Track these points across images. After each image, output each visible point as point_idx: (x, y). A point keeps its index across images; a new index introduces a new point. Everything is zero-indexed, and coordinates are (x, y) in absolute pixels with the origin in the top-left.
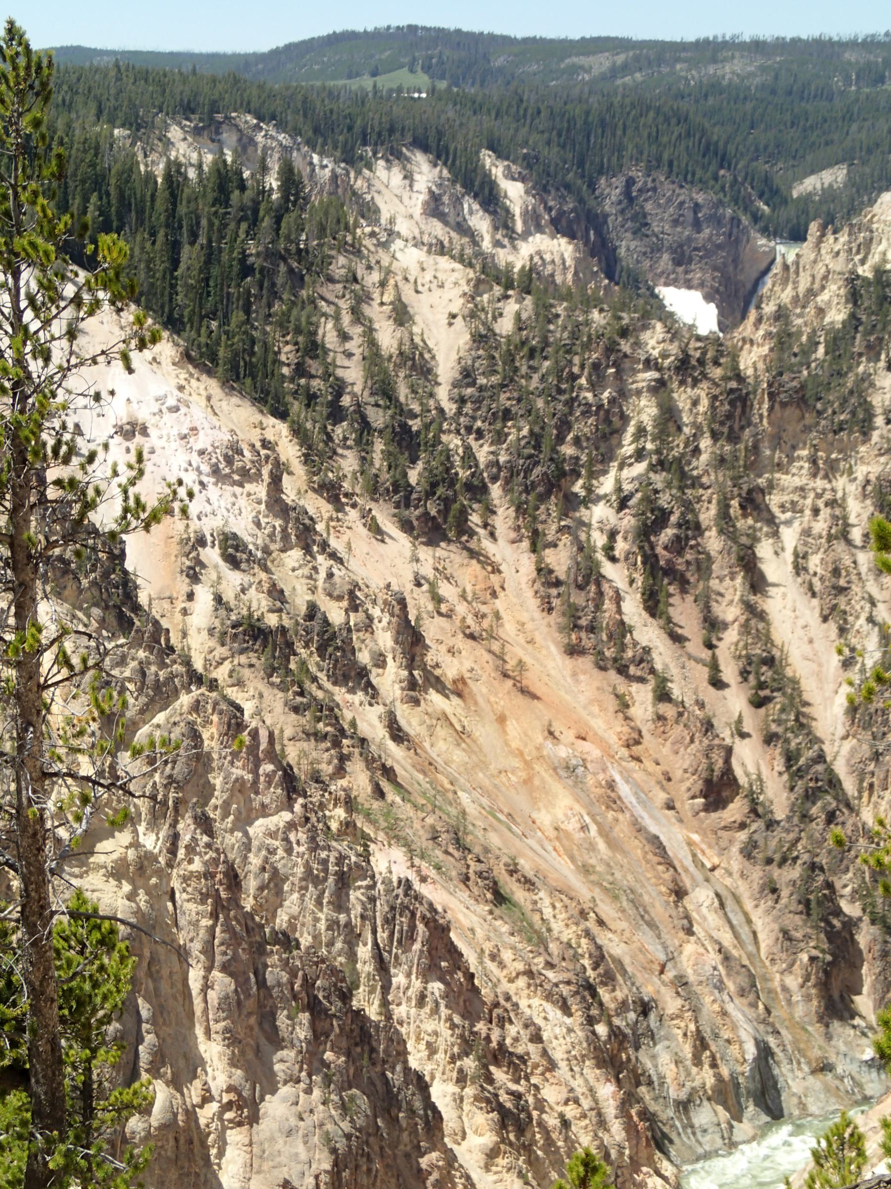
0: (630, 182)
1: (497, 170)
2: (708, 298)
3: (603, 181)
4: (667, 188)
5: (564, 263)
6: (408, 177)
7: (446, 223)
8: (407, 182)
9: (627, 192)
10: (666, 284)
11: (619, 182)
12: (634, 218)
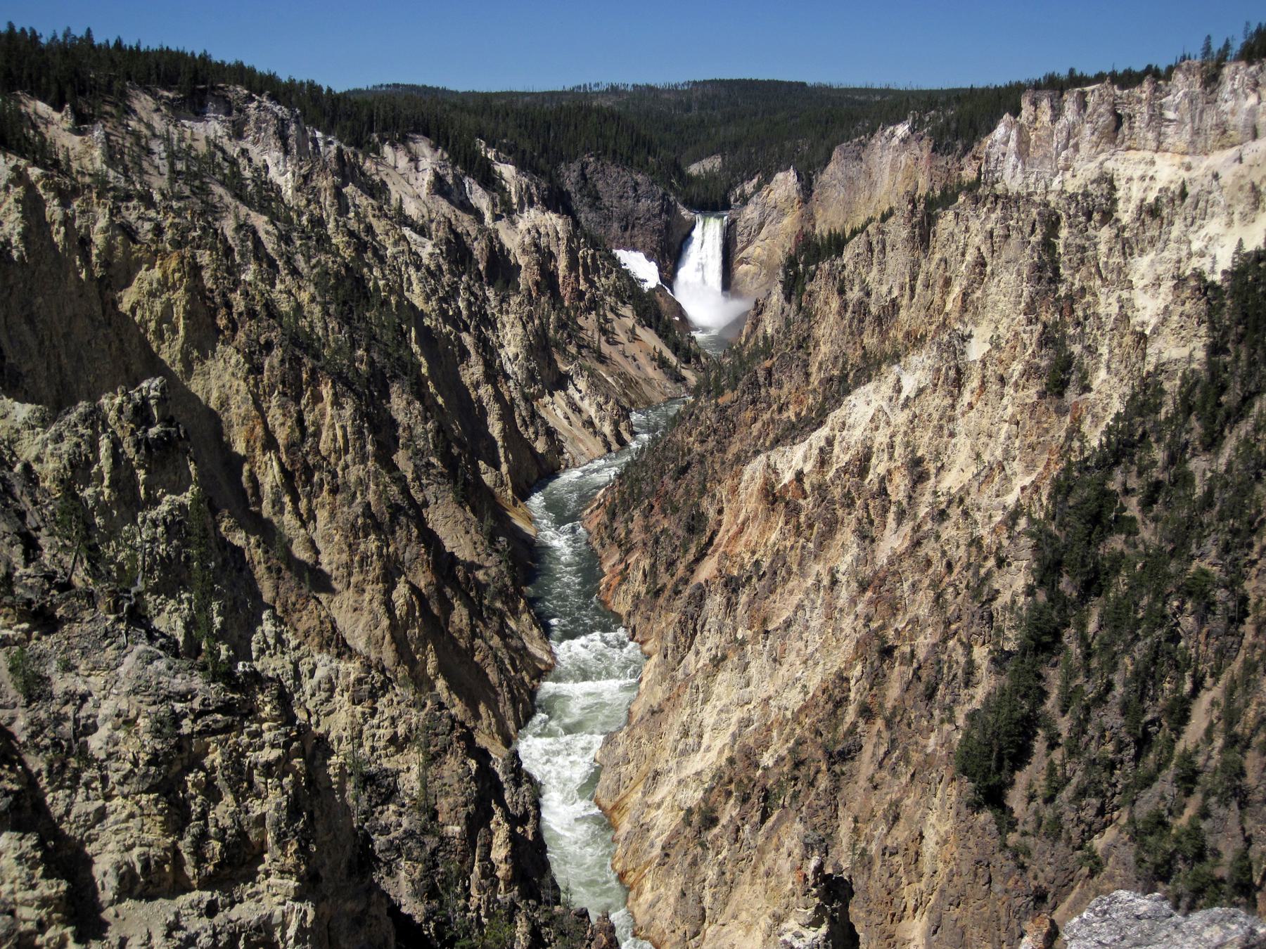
0: (584, 167)
1: (491, 155)
2: (649, 257)
3: (563, 165)
4: (613, 170)
5: (557, 233)
6: (414, 159)
7: (451, 202)
8: (413, 164)
9: (583, 175)
10: (618, 248)
11: (576, 166)
12: (589, 196)
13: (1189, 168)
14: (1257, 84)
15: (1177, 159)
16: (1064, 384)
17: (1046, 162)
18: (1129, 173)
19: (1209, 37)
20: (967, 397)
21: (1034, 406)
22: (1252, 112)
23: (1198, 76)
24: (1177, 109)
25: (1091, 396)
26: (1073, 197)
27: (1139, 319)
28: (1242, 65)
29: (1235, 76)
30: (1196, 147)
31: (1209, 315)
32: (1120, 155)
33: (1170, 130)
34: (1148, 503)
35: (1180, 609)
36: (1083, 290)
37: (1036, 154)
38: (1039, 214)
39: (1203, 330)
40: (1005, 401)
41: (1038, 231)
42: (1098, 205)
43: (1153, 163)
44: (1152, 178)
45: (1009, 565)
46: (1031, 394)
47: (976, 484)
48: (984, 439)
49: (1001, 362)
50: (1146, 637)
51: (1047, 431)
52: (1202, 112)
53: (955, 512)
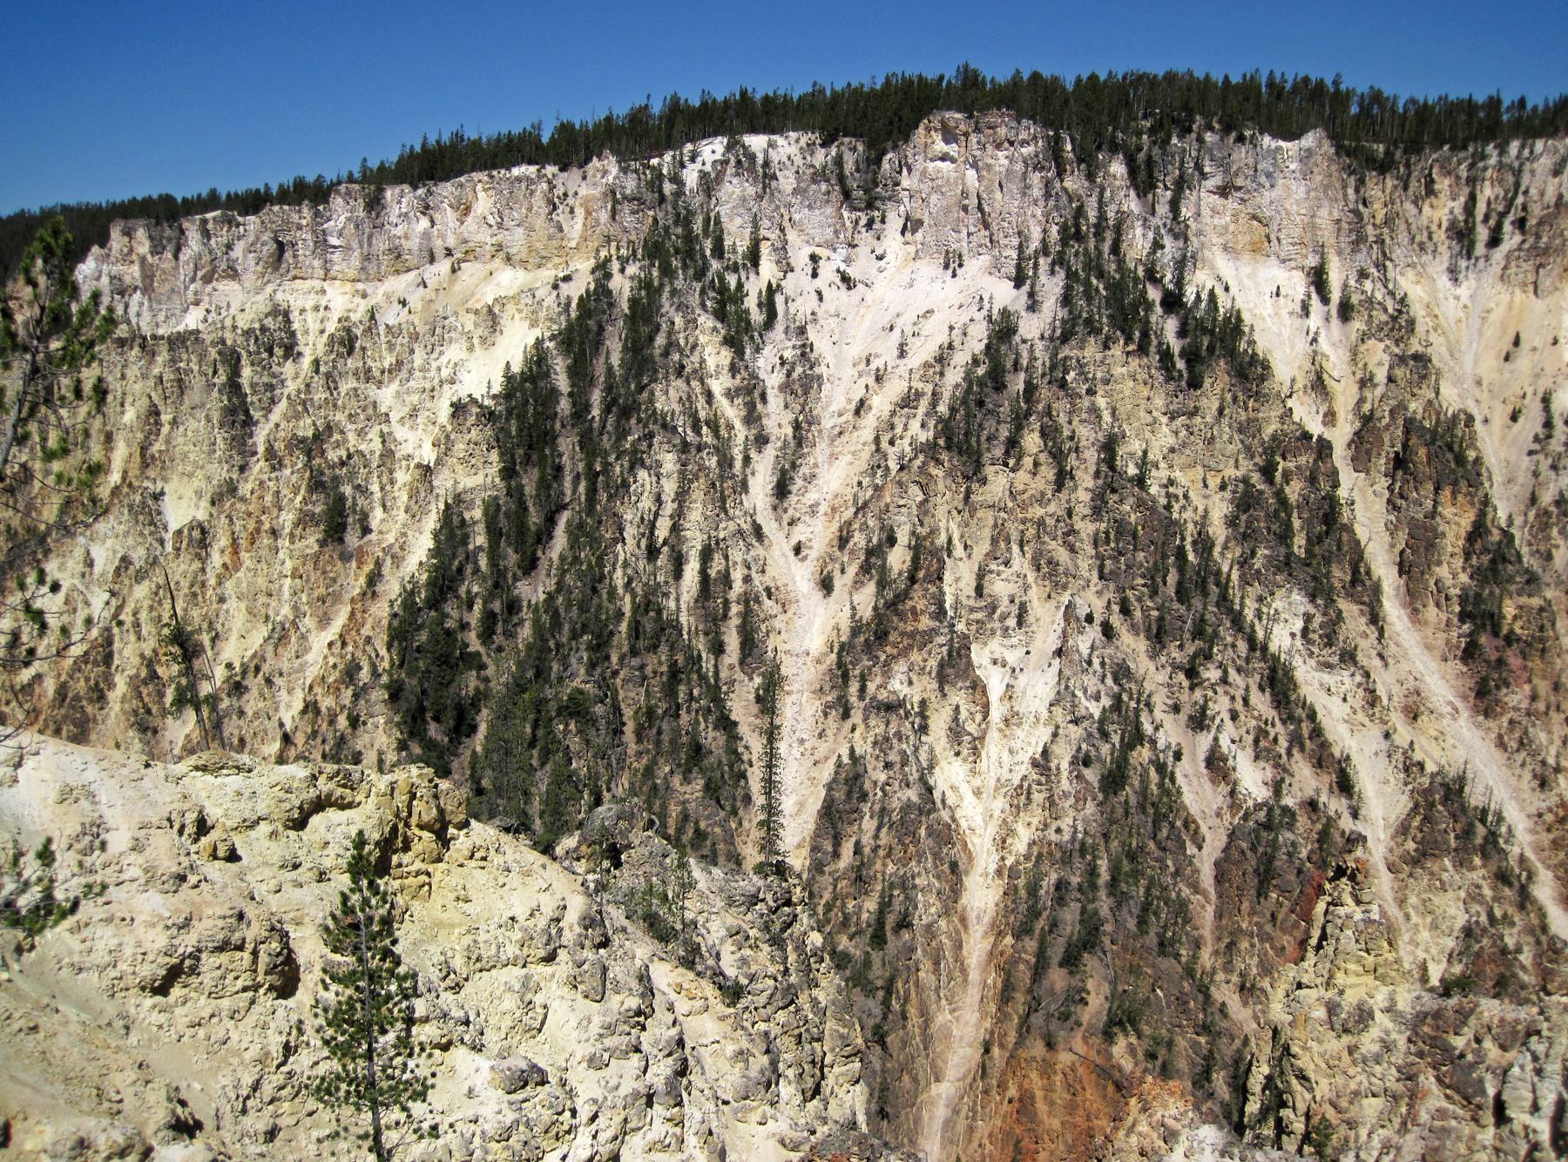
13: (364, 296)
14: (427, 207)
15: (348, 287)
16: (342, 527)
17: (175, 297)
18: (300, 304)
19: (365, 160)
20: (216, 560)
21: (316, 558)
22: (426, 235)
23: (361, 201)
24: (340, 235)
25: (373, 537)
26: (248, 333)
27: (404, 453)
28: (406, 188)
29: (400, 200)
30: (369, 271)
31: (498, 440)
32: (287, 285)
33: (336, 257)
34: (487, 635)
35: (566, 731)
36: (329, 428)
37: (161, 288)
38: (220, 353)
39: (494, 456)
40: (281, 555)
41: (221, 371)
42: (277, 339)
43: (323, 292)
44: (326, 308)
45: (364, 723)
46: (311, 542)
47: (270, 648)
48: (262, 599)
49: (249, 514)
50: (543, 764)
51: (334, 580)
52: (370, 237)
53: (254, 683)
